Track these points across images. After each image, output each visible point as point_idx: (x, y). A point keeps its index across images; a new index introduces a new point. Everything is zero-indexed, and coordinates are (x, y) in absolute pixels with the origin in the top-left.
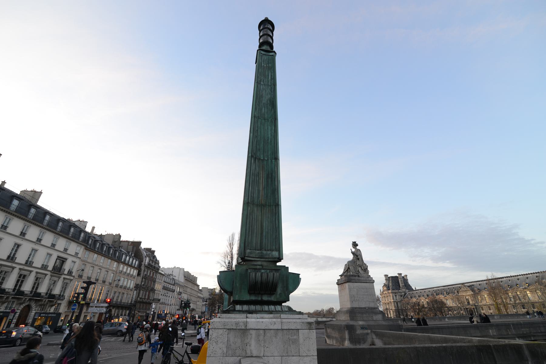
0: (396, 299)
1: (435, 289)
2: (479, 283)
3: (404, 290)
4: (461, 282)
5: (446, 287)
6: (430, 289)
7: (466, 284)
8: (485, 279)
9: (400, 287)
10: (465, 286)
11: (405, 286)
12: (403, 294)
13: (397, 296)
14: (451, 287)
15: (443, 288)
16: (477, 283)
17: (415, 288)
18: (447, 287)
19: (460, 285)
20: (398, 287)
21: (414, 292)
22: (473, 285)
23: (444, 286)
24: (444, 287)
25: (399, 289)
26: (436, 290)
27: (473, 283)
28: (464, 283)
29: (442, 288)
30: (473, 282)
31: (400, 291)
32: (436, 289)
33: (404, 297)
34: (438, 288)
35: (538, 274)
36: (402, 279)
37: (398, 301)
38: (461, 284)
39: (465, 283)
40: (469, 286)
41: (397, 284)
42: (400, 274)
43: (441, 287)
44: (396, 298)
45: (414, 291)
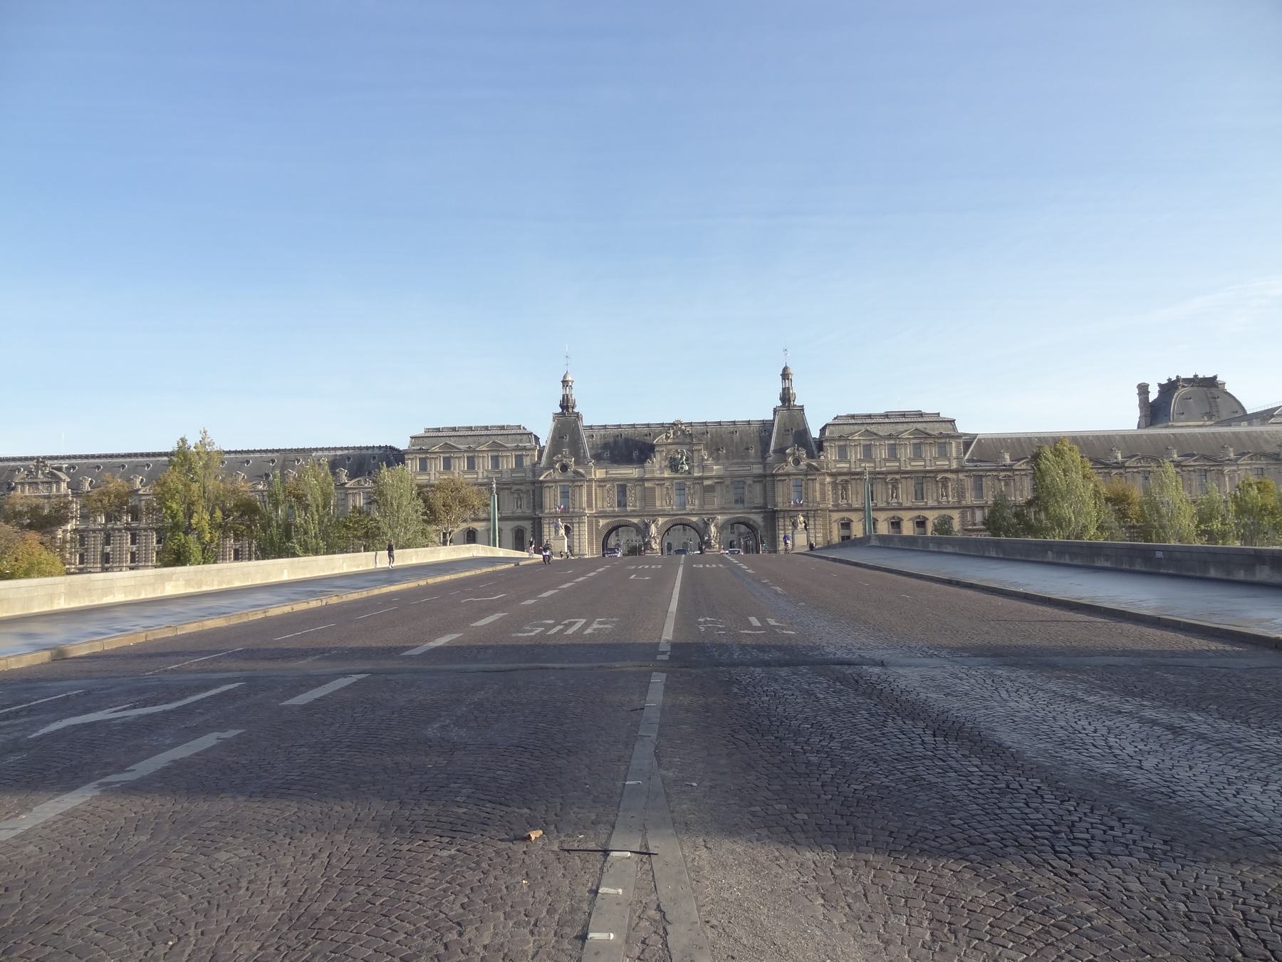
8: (170, 450)
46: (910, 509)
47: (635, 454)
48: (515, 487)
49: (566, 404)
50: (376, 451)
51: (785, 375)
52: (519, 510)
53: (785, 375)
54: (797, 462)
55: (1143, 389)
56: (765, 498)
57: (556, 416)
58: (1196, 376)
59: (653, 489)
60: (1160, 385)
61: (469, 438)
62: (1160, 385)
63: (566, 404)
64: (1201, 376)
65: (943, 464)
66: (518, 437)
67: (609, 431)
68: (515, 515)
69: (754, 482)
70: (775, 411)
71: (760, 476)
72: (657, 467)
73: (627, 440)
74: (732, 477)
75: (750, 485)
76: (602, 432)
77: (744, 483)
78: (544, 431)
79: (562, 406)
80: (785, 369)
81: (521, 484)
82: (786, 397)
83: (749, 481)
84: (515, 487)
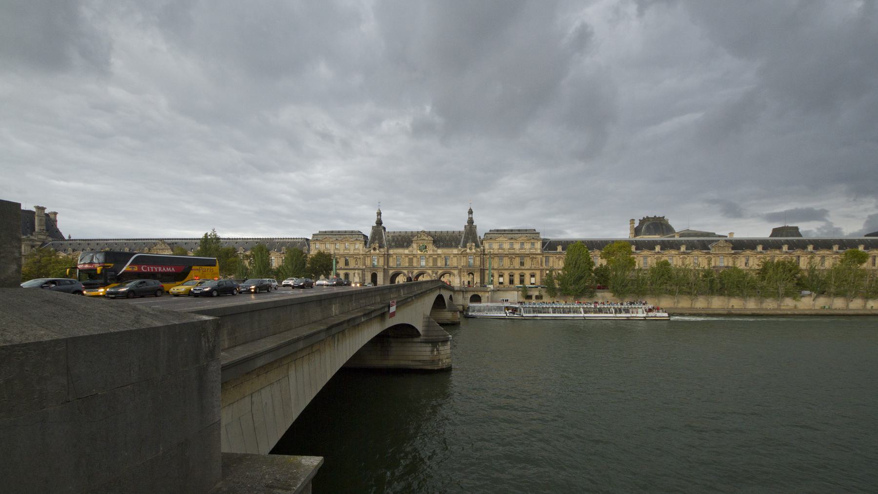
1: (110, 241)
2: (186, 241)
3: (43, 237)
4: (159, 238)
5: (131, 241)
7: (167, 241)
9: (34, 230)
10: (164, 243)
14: (140, 241)
15: (126, 241)
16: (183, 241)
17: (70, 237)
19: (157, 241)
21: (64, 242)
22: (176, 243)
24: (128, 241)
26: (112, 243)
27: (176, 241)
28: (163, 239)
30: (178, 239)
32: (112, 241)
34: (117, 241)
35: (259, 240)
36: (44, 218)
38: (158, 239)
39: (166, 239)
40: (169, 244)
42: (43, 209)
43: (123, 240)
45: (66, 240)
46: (518, 269)
47: (405, 244)
48: (355, 256)
49: (379, 222)
50: (300, 240)
51: (471, 212)
52: (357, 266)
53: (471, 212)
54: (471, 249)
55: (632, 221)
56: (458, 264)
57: (373, 227)
58: (655, 216)
59: (412, 259)
60: (640, 220)
61: (337, 236)
62: (640, 220)
63: (379, 222)
64: (657, 216)
65: (533, 251)
66: (357, 236)
67: (395, 234)
68: (355, 268)
69: (454, 257)
70: (465, 227)
71: (456, 254)
72: (414, 249)
73: (403, 237)
74: (444, 254)
75: (452, 258)
76: (392, 234)
77: (450, 257)
78: (368, 232)
79: (377, 223)
80: (470, 209)
81: (358, 255)
82: (471, 221)
83: (452, 256)
84: (355, 256)
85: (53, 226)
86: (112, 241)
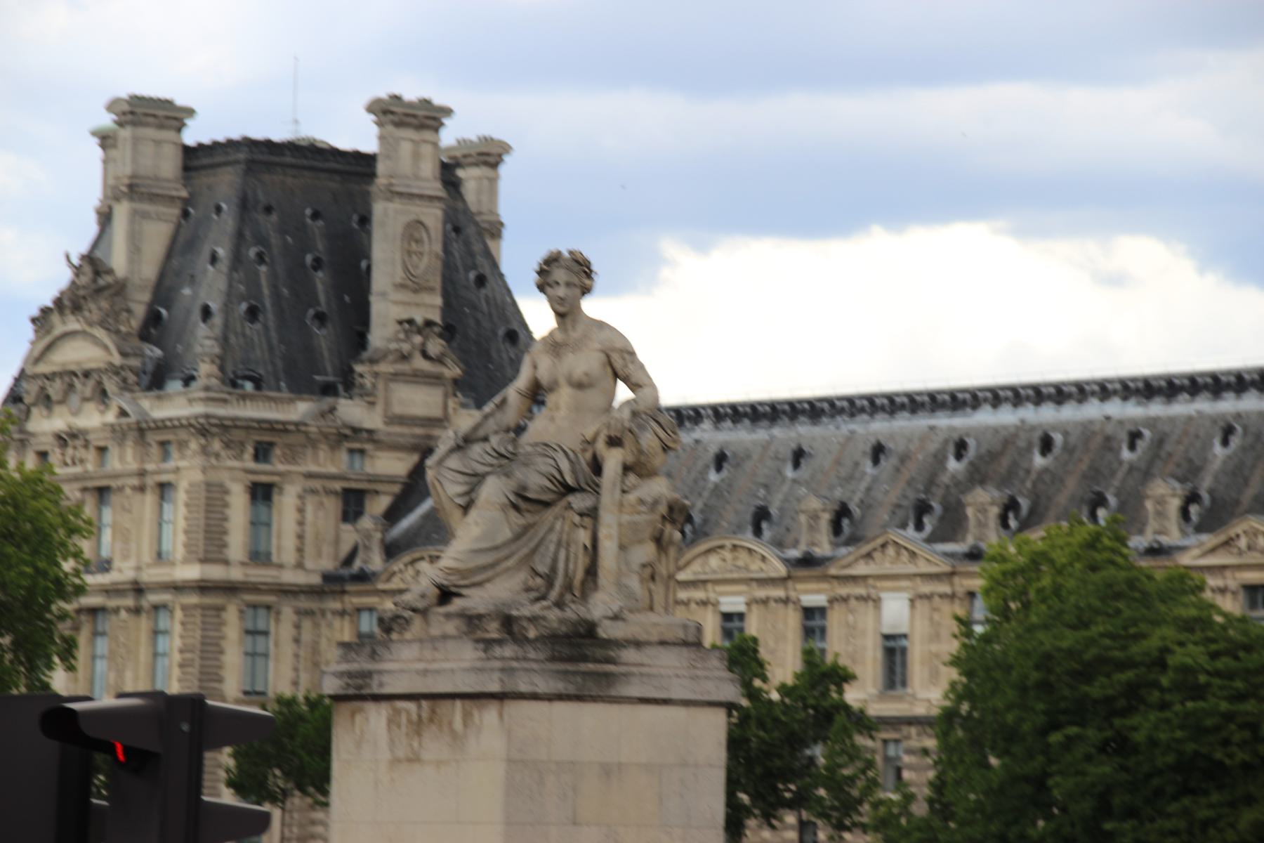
0: (258, 556)
1: (985, 417)
5: (1182, 408)
6: (904, 424)
11: (449, 331)
12: (395, 465)
13: (287, 502)
15: (1132, 410)
18: (1203, 405)
20: (324, 338)
23: (1147, 389)
24: (1157, 409)
25: (346, 383)
26: (1008, 440)
29: (1116, 408)
31: (351, 411)
32: (1007, 417)
33: (392, 515)
34: (1047, 414)
37: (290, 577)
41: (320, 279)
43: (1104, 390)
44: (259, 525)
85: (481, 281)
86: (1007, 417)
